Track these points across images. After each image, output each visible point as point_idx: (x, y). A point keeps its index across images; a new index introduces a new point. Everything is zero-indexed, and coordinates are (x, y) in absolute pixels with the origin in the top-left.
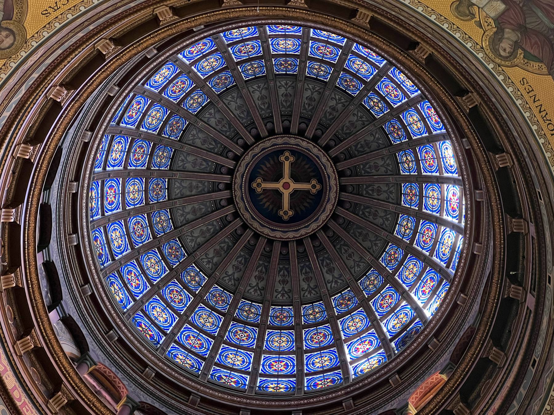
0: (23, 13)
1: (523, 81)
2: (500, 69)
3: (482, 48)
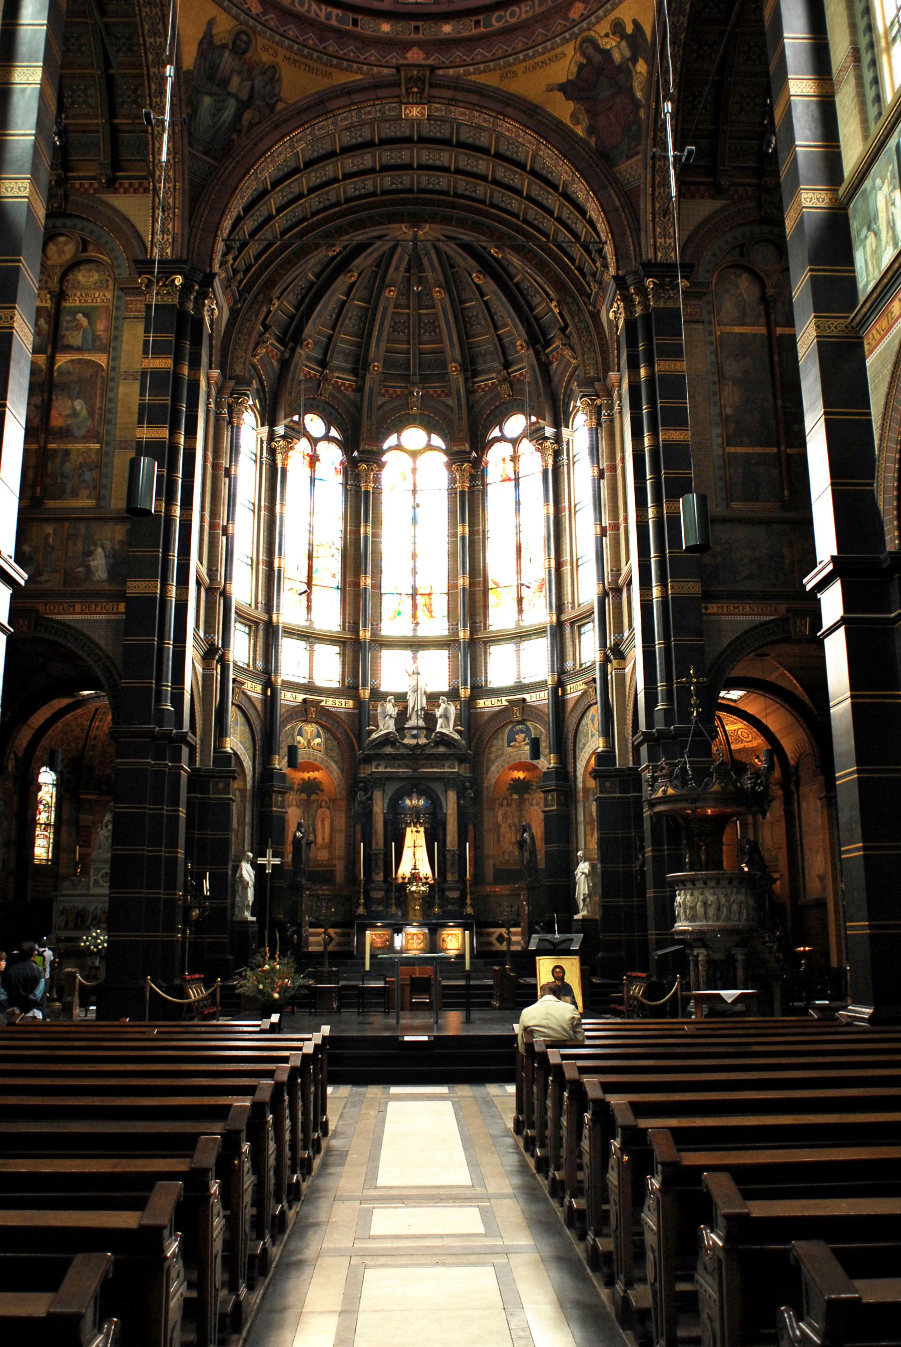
3: (590, 29)
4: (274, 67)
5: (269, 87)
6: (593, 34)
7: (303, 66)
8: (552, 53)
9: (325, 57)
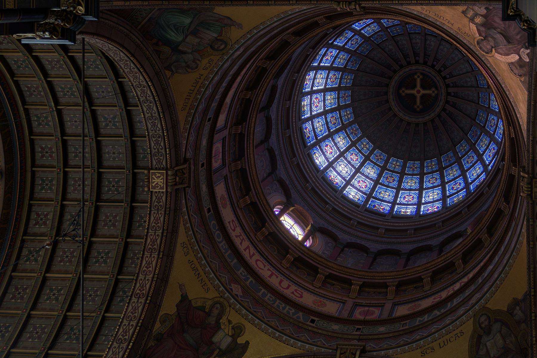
1: (208, 290)
2: (221, 295)
3: (230, 306)
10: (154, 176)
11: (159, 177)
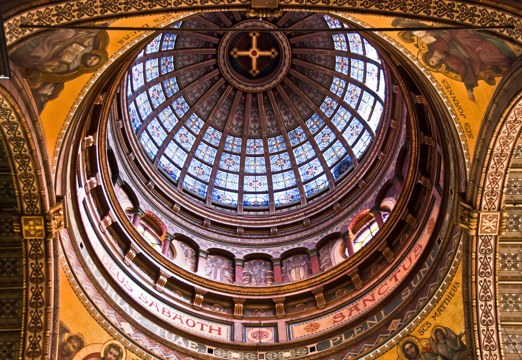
0: (106, 44)
1: (444, 81)
3: (417, 59)
4: (437, 331)
5: (448, 343)
6: (420, 57)
7: (445, 305)
8: (446, 91)
9: (444, 282)
10: (494, 228)
11: (487, 228)
